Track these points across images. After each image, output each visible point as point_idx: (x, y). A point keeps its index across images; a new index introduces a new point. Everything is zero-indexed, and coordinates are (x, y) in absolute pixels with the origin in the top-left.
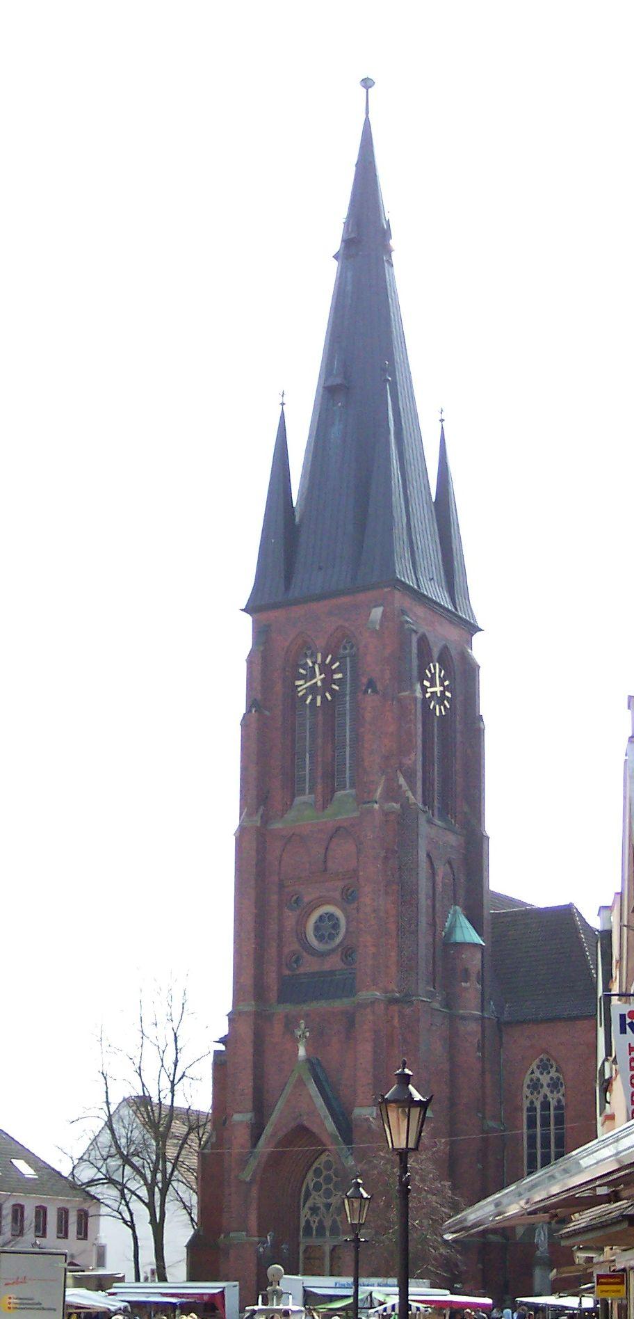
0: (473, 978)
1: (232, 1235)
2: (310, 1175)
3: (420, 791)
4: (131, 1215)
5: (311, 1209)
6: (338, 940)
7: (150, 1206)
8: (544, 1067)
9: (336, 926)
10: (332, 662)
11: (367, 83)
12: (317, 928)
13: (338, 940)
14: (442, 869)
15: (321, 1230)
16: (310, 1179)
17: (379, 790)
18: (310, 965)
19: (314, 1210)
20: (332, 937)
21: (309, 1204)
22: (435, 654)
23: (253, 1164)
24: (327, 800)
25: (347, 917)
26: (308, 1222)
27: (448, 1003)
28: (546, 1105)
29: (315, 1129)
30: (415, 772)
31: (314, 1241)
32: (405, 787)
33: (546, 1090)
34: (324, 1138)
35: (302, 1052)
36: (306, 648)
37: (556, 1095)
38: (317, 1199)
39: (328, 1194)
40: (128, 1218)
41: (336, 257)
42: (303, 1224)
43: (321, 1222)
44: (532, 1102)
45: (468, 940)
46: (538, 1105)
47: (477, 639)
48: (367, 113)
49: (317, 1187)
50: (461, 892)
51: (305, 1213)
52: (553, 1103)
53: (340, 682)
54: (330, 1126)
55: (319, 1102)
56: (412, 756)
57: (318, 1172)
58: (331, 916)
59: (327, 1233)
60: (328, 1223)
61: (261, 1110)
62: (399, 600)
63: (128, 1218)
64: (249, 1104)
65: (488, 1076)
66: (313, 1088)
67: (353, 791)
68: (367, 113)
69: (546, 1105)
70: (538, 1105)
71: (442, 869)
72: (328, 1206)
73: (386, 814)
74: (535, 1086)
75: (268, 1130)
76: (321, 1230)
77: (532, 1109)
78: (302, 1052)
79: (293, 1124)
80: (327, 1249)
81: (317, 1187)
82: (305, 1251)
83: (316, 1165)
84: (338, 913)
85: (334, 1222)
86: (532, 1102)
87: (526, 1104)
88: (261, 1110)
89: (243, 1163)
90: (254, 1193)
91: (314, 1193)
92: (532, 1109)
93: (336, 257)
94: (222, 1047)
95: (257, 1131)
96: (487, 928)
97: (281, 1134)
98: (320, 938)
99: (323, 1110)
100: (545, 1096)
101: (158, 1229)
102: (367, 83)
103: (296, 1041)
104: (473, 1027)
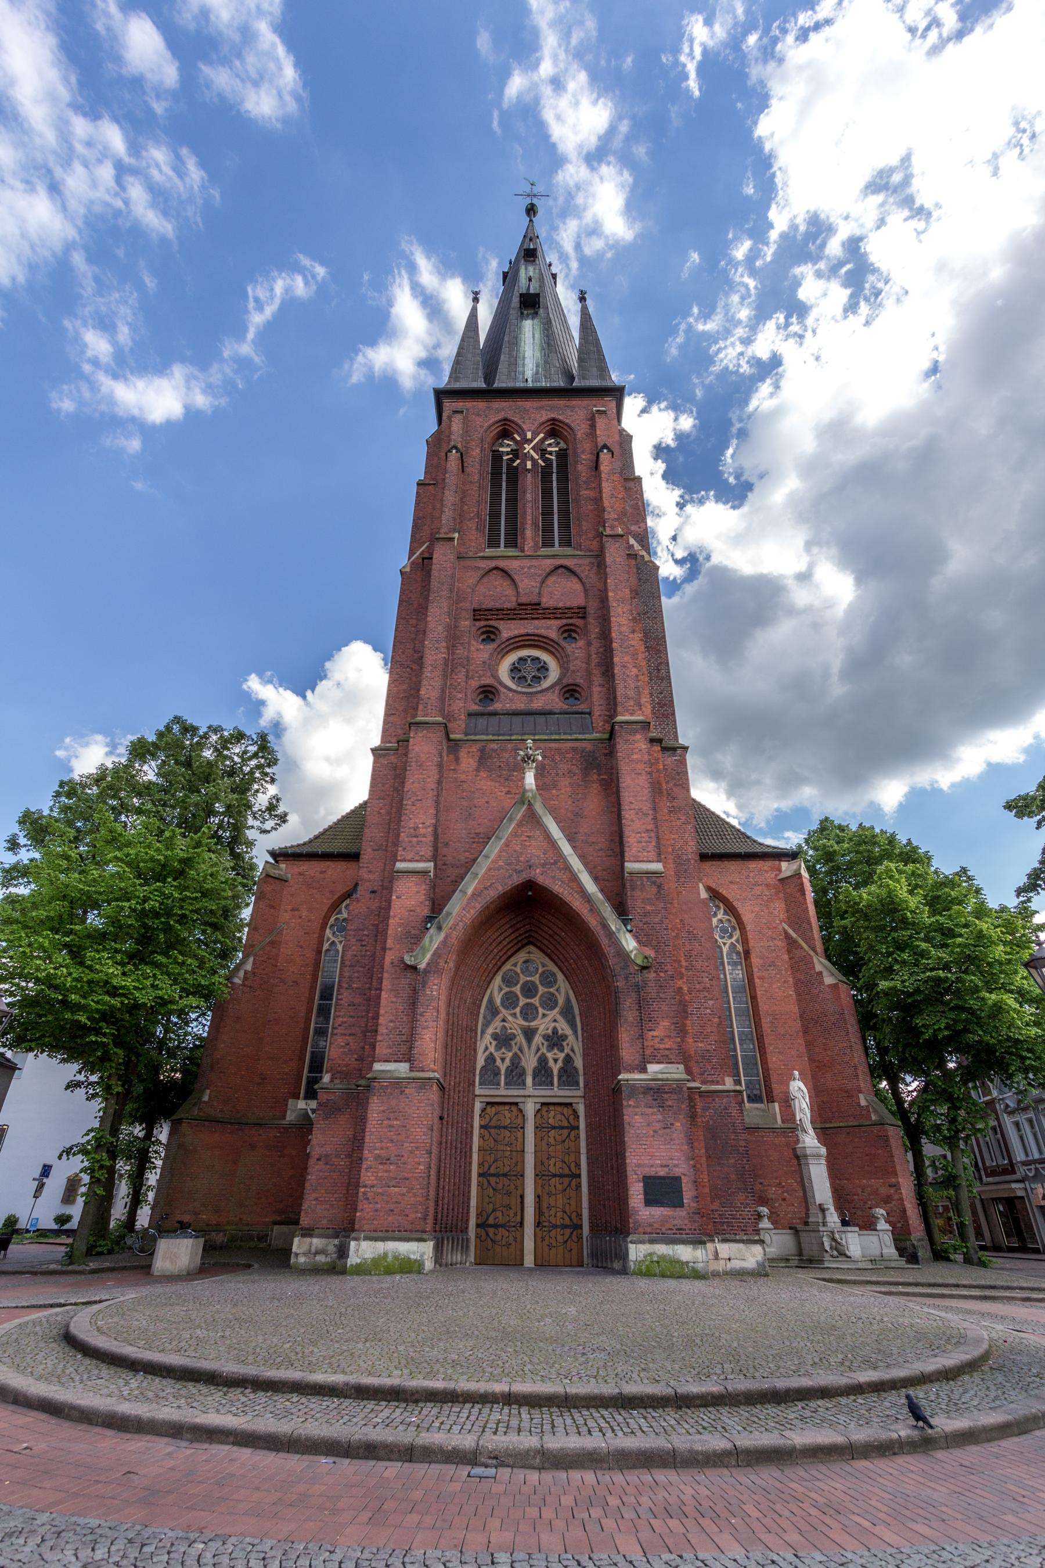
2: (498, 980)
5: (495, 1037)
9: (544, 668)
15: (516, 1076)
16: (496, 990)
19: (504, 1040)
26: (491, 1059)
29: (558, 888)
34: (577, 904)
38: (515, 1023)
39: (529, 1012)
42: (480, 1062)
51: (485, 1044)
57: (509, 981)
59: (529, 1080)
79: (516, 880)
80: (530, 1108)
81: (510, 1001)
83: (508, 966)
85: (543, 1061)
89: (414, 938)
90: (437, 990)
91: (504, 1012)
97: (493, 894)
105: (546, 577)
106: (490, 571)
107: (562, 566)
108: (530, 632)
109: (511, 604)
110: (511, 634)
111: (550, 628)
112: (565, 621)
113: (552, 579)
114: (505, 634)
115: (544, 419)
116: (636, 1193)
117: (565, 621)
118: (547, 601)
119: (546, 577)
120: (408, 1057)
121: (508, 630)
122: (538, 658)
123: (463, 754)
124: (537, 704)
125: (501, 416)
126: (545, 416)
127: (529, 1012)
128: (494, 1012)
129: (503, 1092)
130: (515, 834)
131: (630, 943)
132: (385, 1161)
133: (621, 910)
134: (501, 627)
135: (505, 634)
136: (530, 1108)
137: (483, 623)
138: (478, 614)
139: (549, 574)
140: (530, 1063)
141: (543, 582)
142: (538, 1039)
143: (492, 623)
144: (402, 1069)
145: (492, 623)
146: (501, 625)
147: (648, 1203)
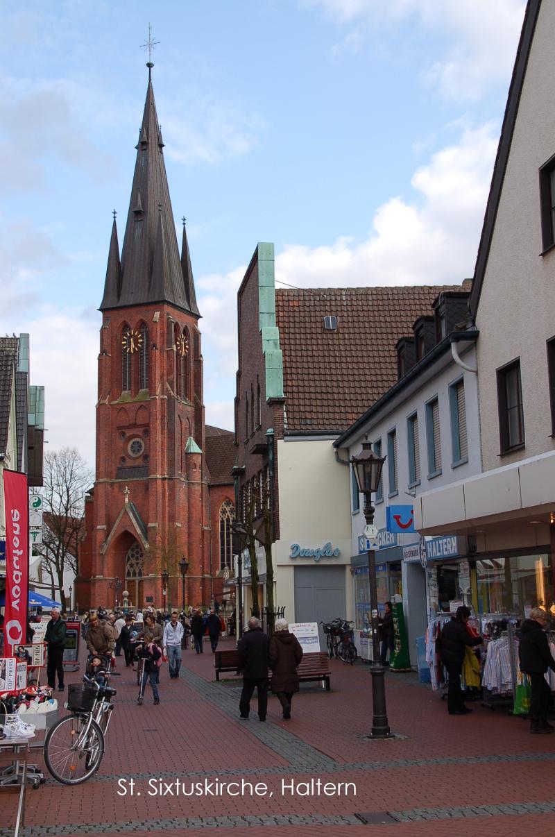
1: (97, 576)
3: (175, 390)
4: (51, 568)
6: (141, 453)
7: (57, 564)
8: (228, 504)
9: (140, 446)
10: (138, 334)
11: (150, 65)
12: (132, 447)
13: (141, 453)
14: (185, 421)
17: (159, 390)
18: (129, 463)
19: (132, 566)
20: (138, 451)
21: (129, 563)
22: (182, 330)
23: (106, 547)
24: (136, 393)
27: (188, 478)
28: (228, 520)
29: (132, 532)
30: (173, 382)
31: (131, 578)
32: (170, 389)
33: (228, 513)
34: (136, 536)
35: (127, 500)
36: (126, 327)
37: (232, 516)
39: (137, 559)
40: (49, 570)
41: (136, 148)
42: (127, 571)
43: (134, 570)
44: (222, 519)
45: (196, 451)
46: (225, 519)
47: (200, 321)
48: (150, 79)
49: (133, 556)
50: (193, 431)
51: (127, 567)
52: (231, 519)
53: (141, 343)
54: (139, 531)
55: (134, 521)
56: (172, 376)
57: (133, 550)
60: (137, 571)
61: (110, 525)
62: (167, 308)
63: (49, 570)
64: (104, 522)
65: (204, 508)
66: (131, 515)
67: (147, 390)
68: (150, 79)
69: (228, 520)
70: (225, 519)
71: (185, 421)
72: (137, 564)
73: (162, 399)
74: (224, 512)
75: (112, 533)
76: (134, 575)
77: (222, 521)
78: (127, 500)
79: (123, 530)
80: (137, 582)
81: (133, 556)
82: (128, 583)
83: (132, 547)
84: (141, 441)
86: (222, 519)
87: (220, 519)
88: (110, 525)
92: (222, 521)
93: (136, 148)
94: (89, 495)
95: (108, 533)
96: (203, 446)
97: (119, 533)
98: (134, 451)
99: (136, 525)
100: (228, 516)
101: (60, 573)
102: (150, 65)
103: (125, 494)
104: (198, 488)
109: (127, 424)
111: (139, 431)
113: (140, 411)
114: (128, 435)
115: (137, 320)
116: (145, 600)
118: (139, 422)
120: (102, 574)
121: (129, 433)
123: (115, 487)
124: (136, 464)
125: (123, 320)
126: (137, 318)
127: (137, 559)
128: (129, 559)
129: (131, 578)
130: (123, 517)
131: (147, 546)
132: (99, 595)
133: (146, 538)
135: (128, 435)
136: (137, 582)
138: (118, 428)
140: (137, 571)
141: (137, 414)
142: (139, 565)
144: (101, 577)
146: (126, 431)
147: (147, 601)
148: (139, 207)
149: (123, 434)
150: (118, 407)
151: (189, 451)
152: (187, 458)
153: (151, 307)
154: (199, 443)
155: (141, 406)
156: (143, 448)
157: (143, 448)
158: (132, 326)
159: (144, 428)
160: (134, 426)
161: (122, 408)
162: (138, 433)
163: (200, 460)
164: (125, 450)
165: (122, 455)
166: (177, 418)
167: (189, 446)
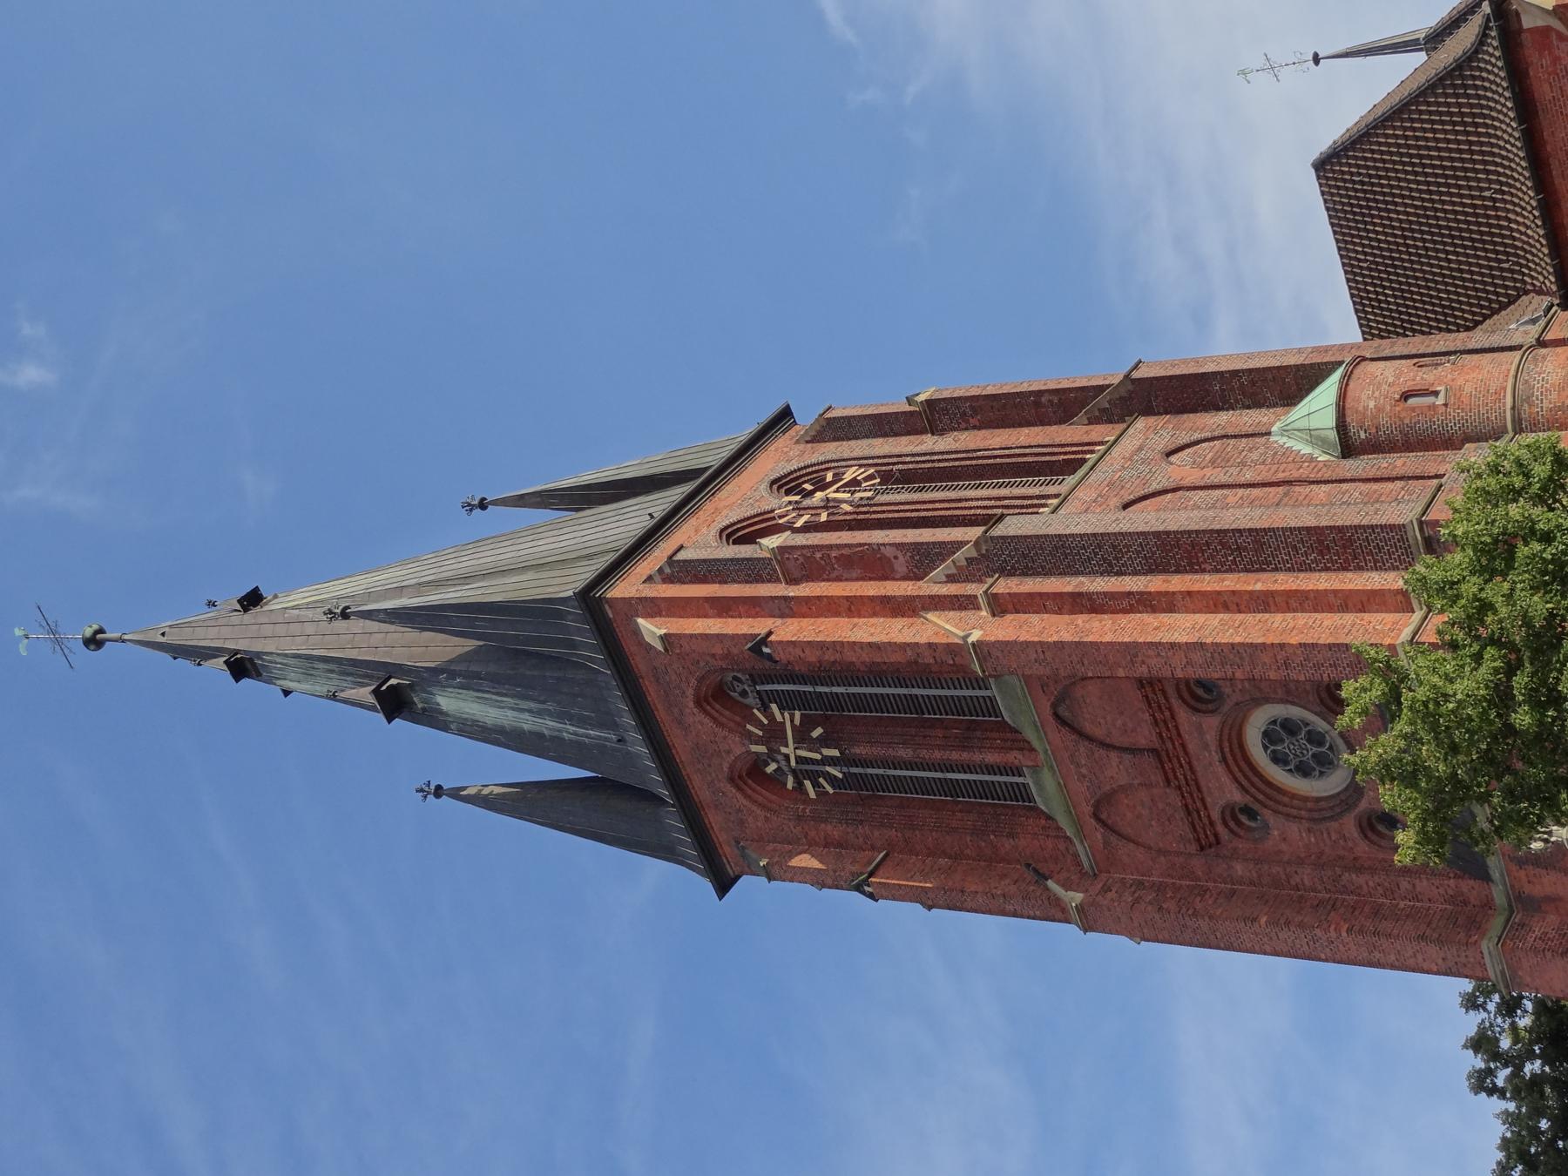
0: (1425, 377)
9: (1290, 727)
12: (1303, 771)
14: (1182, 469)
25: (1258, 702)
56: (889, 552)
58: (1269, 737)
71: (1182, 469)
105: (1090, 739)
106: (1104, 824)
107: (1056, 715)
108: (1216, 757)
110: (1226, 779)
111: (1200, 733)
112: (1175, 702)
113: (1089, 728)
117: (1175, 702)
118: (1145, 735)
119: (1090, 739)
121: (1223, 791)
122: (1266, 734)
123: (1537, 890)
126: (700, 722)
134: (1222, 802)
135: (1237, 797)
137: (1220, 828)
138: (1207, 843)
139: (1081, 734)
143: (1216, 815)
145: (1216, 815)
148: (365, 693)
149: (1232, 814)
150: (1099, 835)
151: (1333, 435)
152: (1375, 446)
153: (640, 664)
154: (1285, 384)
155: (1062, 721)
156: (1295, 712)
157: (1295, 712)
158: (738, 751)
159: (1184, 716)
160: (1168, 758)
161: (1096, 816)
162: (1211, 737)
163: (1386, 371)
164: (1320, 812)
165: (1349, 824)
166: (1145, 519)
167: (1313, 437)
